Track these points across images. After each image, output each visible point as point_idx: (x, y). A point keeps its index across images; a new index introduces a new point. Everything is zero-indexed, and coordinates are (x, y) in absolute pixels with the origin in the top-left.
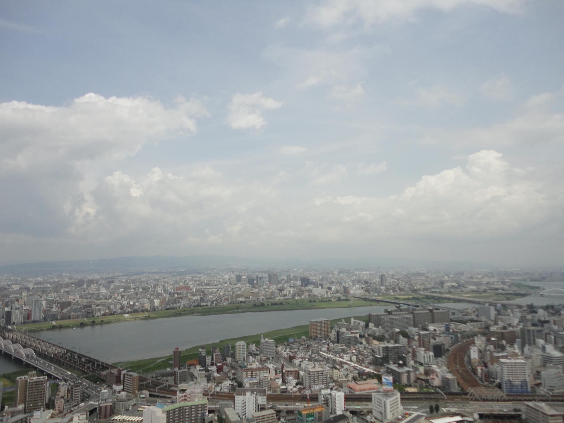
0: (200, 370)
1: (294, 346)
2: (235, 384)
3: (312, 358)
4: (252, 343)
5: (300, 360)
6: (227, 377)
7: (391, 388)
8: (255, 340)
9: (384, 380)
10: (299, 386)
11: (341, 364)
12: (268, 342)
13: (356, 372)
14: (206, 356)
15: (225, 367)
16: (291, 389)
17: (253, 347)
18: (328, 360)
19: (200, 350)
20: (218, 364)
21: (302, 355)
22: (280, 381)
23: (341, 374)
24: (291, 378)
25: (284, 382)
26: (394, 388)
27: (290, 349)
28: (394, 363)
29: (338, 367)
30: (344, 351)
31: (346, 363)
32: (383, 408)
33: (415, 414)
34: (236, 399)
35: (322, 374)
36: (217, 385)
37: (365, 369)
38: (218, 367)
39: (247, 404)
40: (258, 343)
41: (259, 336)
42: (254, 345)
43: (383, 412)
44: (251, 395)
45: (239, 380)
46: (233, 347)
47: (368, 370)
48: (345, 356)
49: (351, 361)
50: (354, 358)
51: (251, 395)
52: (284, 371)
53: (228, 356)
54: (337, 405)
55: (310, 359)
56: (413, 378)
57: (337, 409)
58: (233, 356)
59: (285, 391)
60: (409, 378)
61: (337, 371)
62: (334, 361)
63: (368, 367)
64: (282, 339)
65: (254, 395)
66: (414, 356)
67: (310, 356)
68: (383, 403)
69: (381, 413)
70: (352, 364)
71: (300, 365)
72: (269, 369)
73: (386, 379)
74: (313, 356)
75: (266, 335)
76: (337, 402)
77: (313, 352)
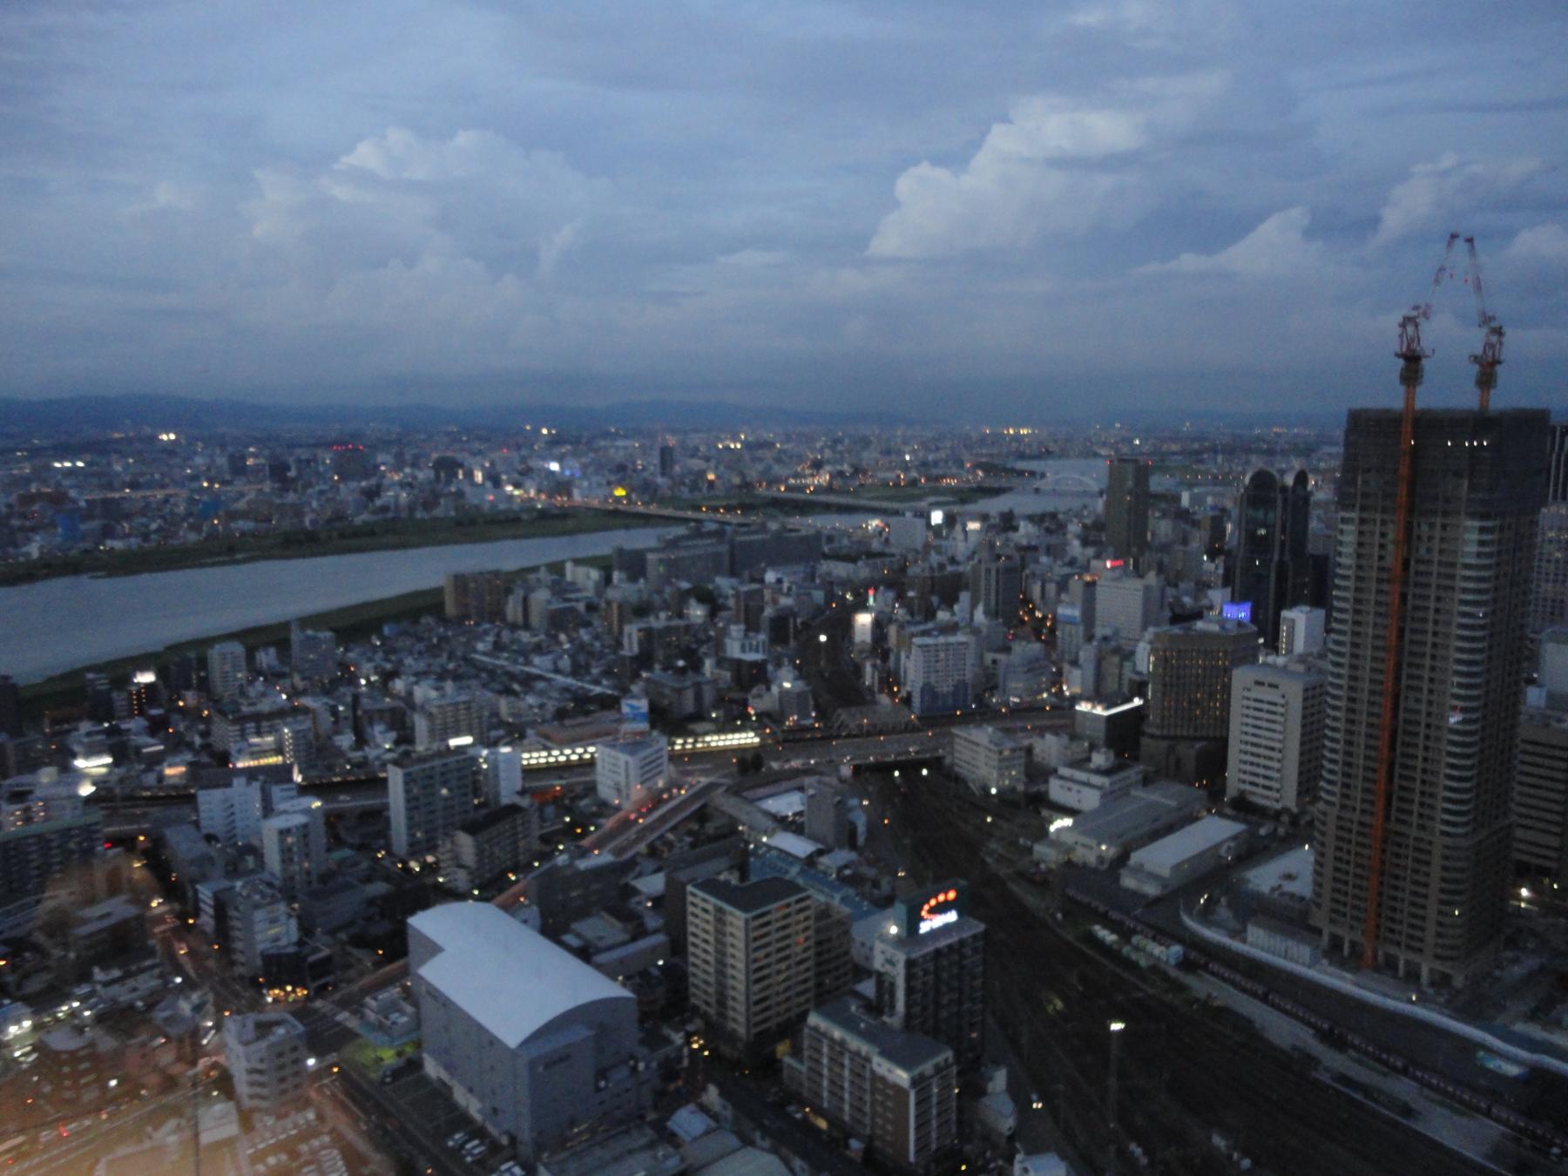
0: (89, 734)
1: (399, 644)
2: (205, 759)
3: (448, 671)
4: (267, 645)
5: (412, 679)
6: (177, 745)
7: (644, 726)
8: (275, 636)
9: (625, 709)
10: (403, 748)
11: (528, 681)
12: (314, 638)
13: (567, 696)
14: (109, 692)
15: (175, 717)
16: (378, 758)
17: (267, 658)
18: (492, 673)
19: (90, 676)
20: (154, 712)
21: (421, 666)
22: (346, 740)
23: (522, 705)
24: (378, 729)
25: (361, 741)
26: (653, 727)
27: (387, 653)
28: (665, 669)
29: (516, 687)
30: (538, 649)
31: (540, 678)
32: (622, 779)
33: (704, 780)
34: (200, 799)
35: (468, 709)
36: (149, 769)
37: (592, 687)
38: (151, 719)
39: (236, 809)
40: (283, 645)
41: (285, 626)
42: (272, 651)
43: (623, 783)
44: (248, 784)
45: (219, 746)
46: (203, 663)
47: (598, 690)
48: (537, 660)
49: (557, 671)
50: (565, 662)
51: (248, 784)
52: (360, 713)
53: (188, 687)
54: (503, 784)
55: (442, 676)
56: (708, 695)
57: (504, 792)
58: (204, 686)
59: (363, 764)
60: (698, 697)
61: (512, 699)
62: (512, 677)
63: (597, 682)
64: (355, 626)
65: (256, 785)
66: (718, 645)
67: (442, 666)
68: (622, 763)
69: (619, 790)
70: (559, 678)
71: (410, 694)
72: (306, 711)
73: (632, 707)
74: (451, 666)
75: (307, 621)
76: (502, 775)
77: (451, 657)
